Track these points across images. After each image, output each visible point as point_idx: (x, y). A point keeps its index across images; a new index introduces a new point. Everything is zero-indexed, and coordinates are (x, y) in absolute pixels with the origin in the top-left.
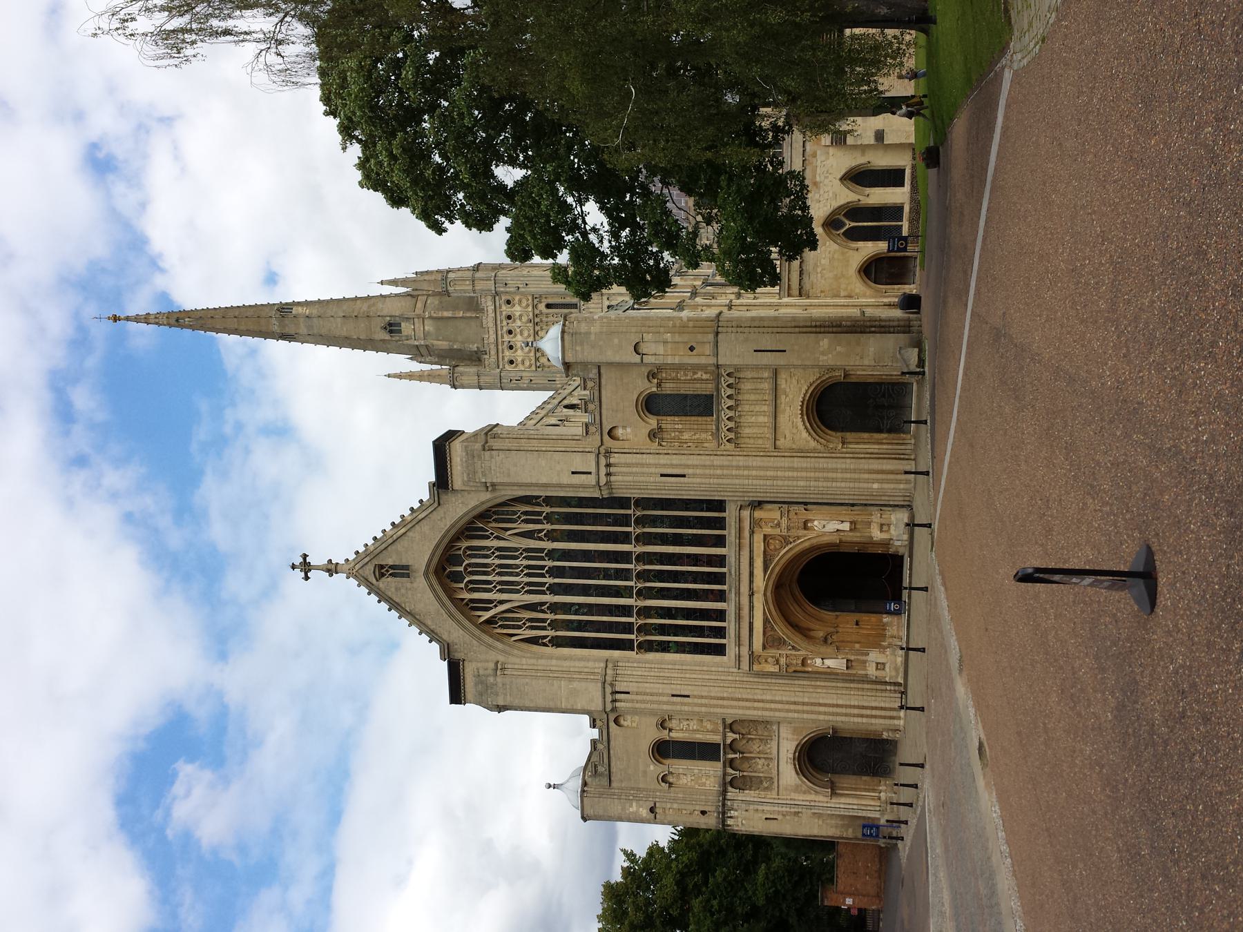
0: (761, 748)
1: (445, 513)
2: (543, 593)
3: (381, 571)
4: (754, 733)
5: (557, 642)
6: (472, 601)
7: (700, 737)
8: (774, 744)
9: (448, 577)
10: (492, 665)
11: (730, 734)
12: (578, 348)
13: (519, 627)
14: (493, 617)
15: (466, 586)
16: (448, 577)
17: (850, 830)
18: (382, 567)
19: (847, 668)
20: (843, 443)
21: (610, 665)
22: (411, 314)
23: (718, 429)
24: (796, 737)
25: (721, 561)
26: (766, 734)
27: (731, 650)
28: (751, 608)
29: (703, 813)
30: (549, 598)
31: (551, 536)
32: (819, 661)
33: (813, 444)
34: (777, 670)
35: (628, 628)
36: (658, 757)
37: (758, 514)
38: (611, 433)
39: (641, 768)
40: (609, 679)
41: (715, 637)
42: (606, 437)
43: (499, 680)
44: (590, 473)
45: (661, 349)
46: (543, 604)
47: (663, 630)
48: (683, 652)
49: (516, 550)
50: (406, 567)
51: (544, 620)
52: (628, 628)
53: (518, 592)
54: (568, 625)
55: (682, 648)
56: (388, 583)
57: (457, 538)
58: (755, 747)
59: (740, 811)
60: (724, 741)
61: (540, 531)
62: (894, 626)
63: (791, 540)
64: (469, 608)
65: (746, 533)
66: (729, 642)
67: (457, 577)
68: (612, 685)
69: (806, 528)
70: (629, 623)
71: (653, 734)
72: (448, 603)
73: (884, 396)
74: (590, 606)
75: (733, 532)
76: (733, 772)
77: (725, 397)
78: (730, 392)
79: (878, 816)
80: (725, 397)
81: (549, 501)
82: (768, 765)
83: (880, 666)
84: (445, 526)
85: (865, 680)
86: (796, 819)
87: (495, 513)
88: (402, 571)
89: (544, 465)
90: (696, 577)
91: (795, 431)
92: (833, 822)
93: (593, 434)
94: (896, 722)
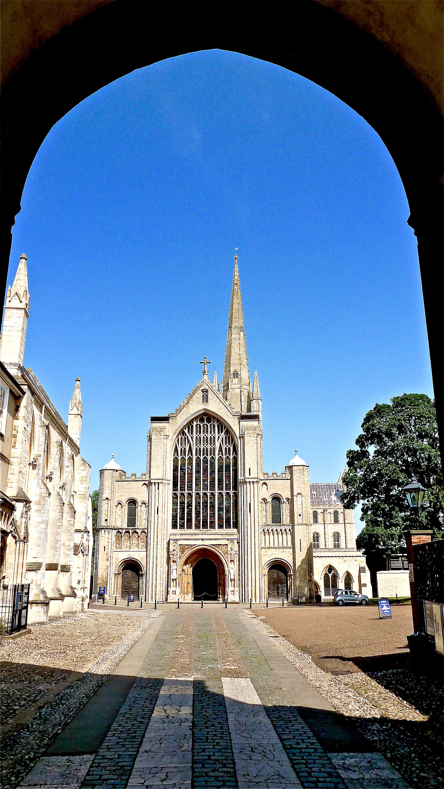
0: (134, 544)
1: (230, 417)
2: (196, 455)
3: (205, 391)
4: (141, 541)
5: (175, 460)
6: (192, 426)
7: (138, 519)
8: (137, 550)
9: (202, 417)
10: (167, 435)
11: (140, 532)
12: (298, 472)
13: (181, 445)
14: (186, 434)
15: (198, 424)
16: (202, 417)
17: (101, 582)
18: (207, 392)
19: (173, 579)
20: (264, 575)
21: (169, 482)
22: (242, 383)
23: (269, 525)
24: (140, 558)
25: (212, 527)
26: (141, 546)
27: (175, 531)
28: (197, 539)
29: (106, 520)
30: (194, 457)
31: (220, 458)
32: (175, 568)
33: (263, 563)
34: (170, 551)
35: (182, 489)
36: (129, 501)
37: (236, 542)
38: (265, 483)
39: (124, 494)
40: (164, 481)
41: (180, 525)
42: (263, 481)
43: (163, 437)
44: (250, 475)
45: (300, 503)
46: (192, 454)
47: (182, 503)
48: (173, 512)
49: (214, 444)
50: (207, 401)
51: (185, 454)
52: (182, 489)
53: (196, 445)
54: (183, 465)
55: (174, 510)
56: (199, 394)
57: (218, 421)
58: (135, 541)
59: (108, 535)
60: (137, 529)
61: (222, 455)
62: (189, 598)
63: (226, 555)
64: (189, 425)
65: (228, 537)
66: (178, 531)
67: (202, 420)
68: (161, 483)
69: (231, 561)
70: (185, 489)
71: (139, 500)
72: (193, 417)
73: (282, 590)
74: (192, 474)
75: (226, 532)
76: (123, 533)
77: (281, 528)
78: (283, 530)
79: (108, 593)
80: (281, 528)
81: (235, 459)
82: (127, 547)
83: (174, 592)
84: (225, 418)
85: (168, 586)
86: (106, 559)
87: (229, 437)
88: (205, 399)
89: (252, 457)
90: (205, 517)
91: (269, 556)
92: (104, 575)
93: (264, 476)
94: (150, 600)
